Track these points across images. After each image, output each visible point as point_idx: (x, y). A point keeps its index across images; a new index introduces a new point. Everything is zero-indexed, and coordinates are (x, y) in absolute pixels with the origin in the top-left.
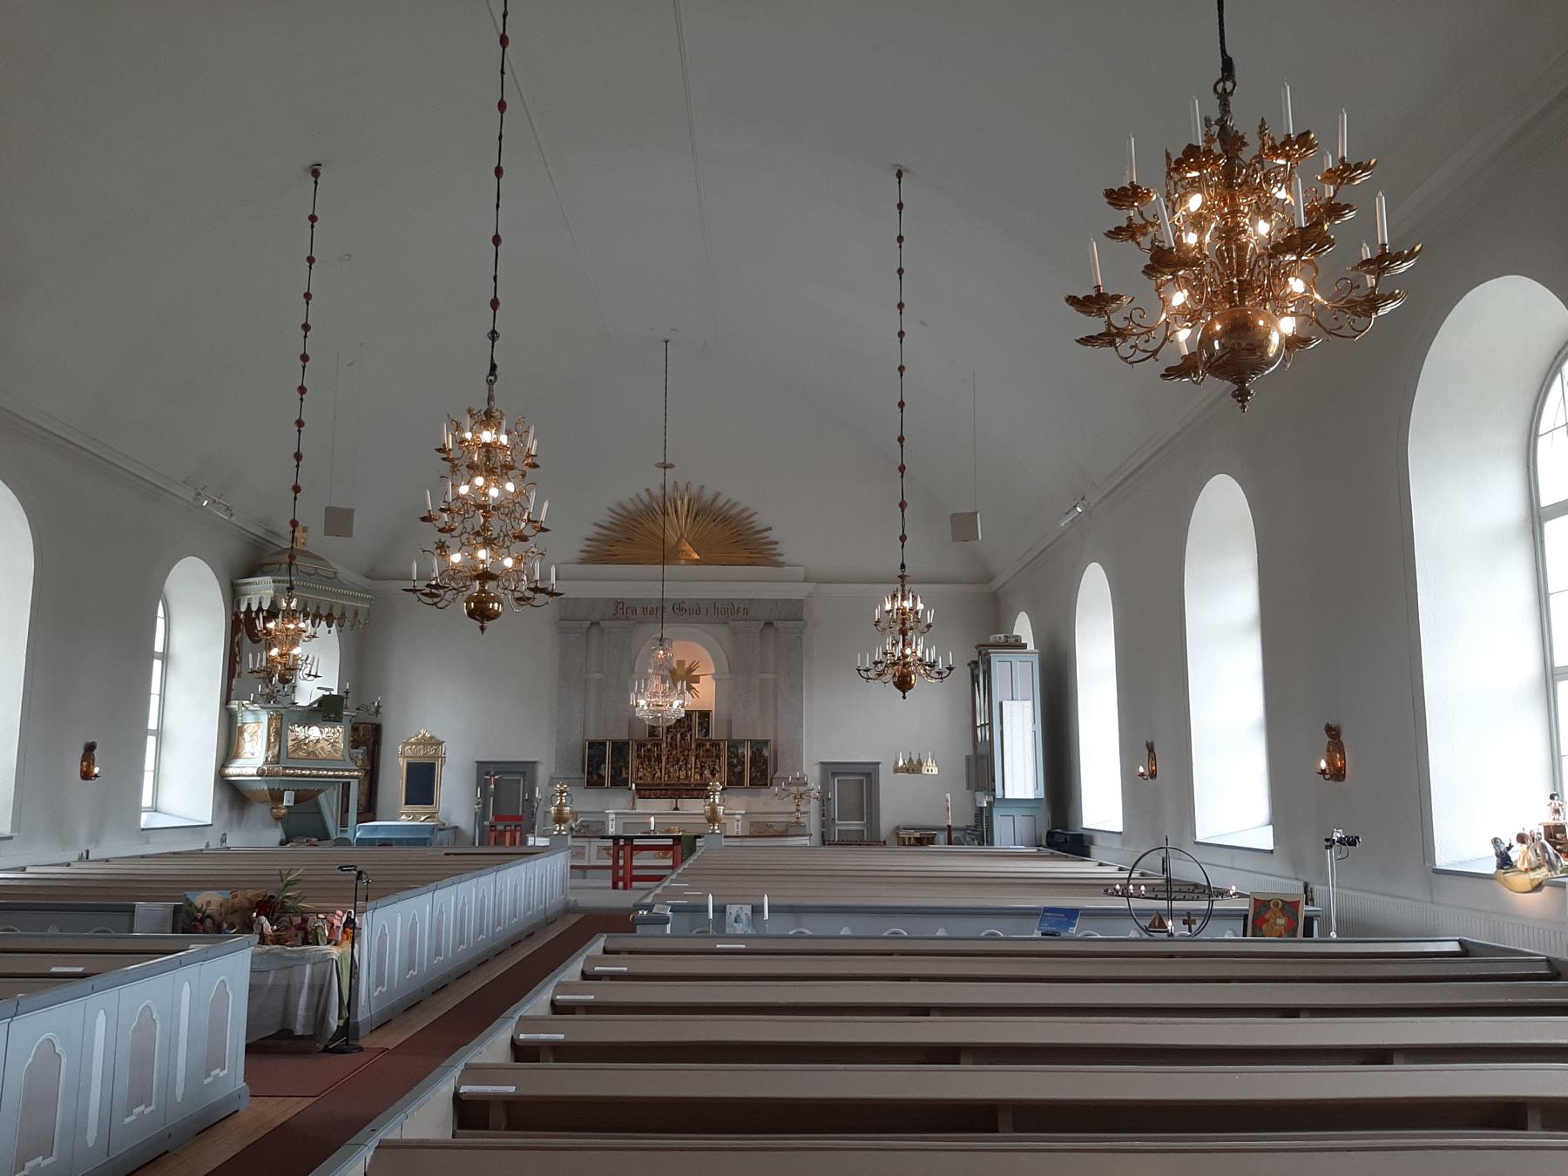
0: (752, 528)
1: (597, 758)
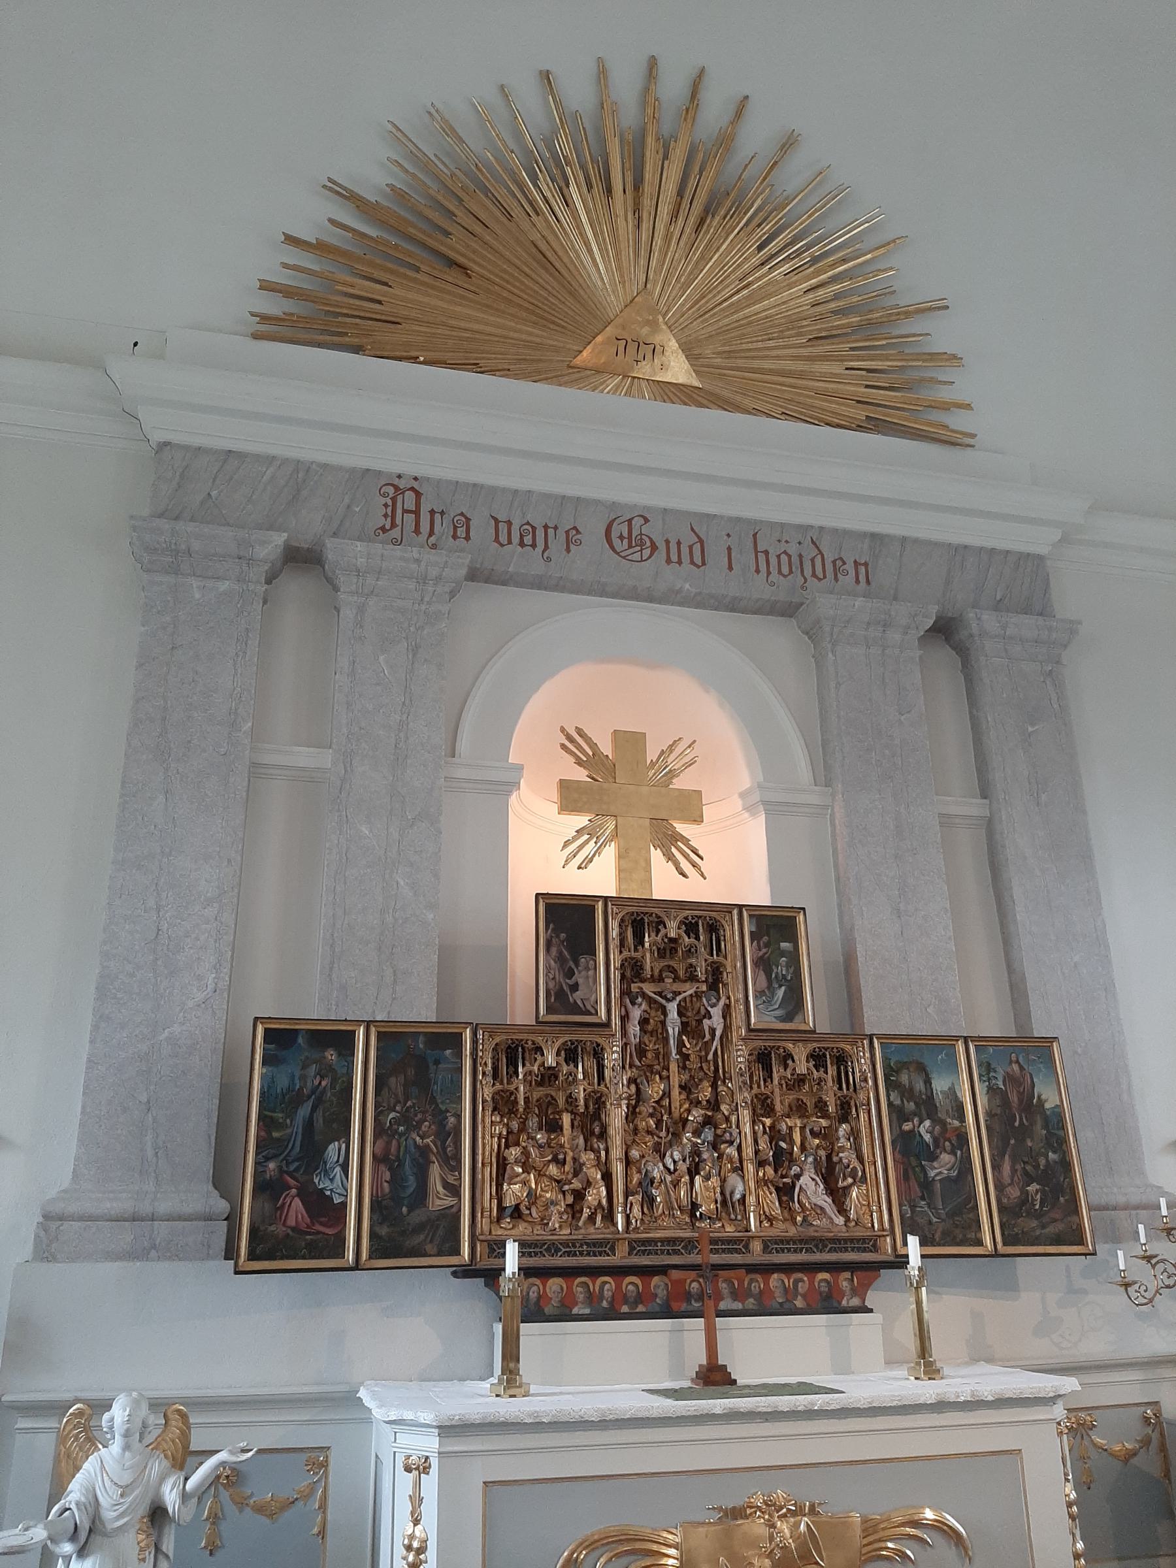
1: (304, 1111)
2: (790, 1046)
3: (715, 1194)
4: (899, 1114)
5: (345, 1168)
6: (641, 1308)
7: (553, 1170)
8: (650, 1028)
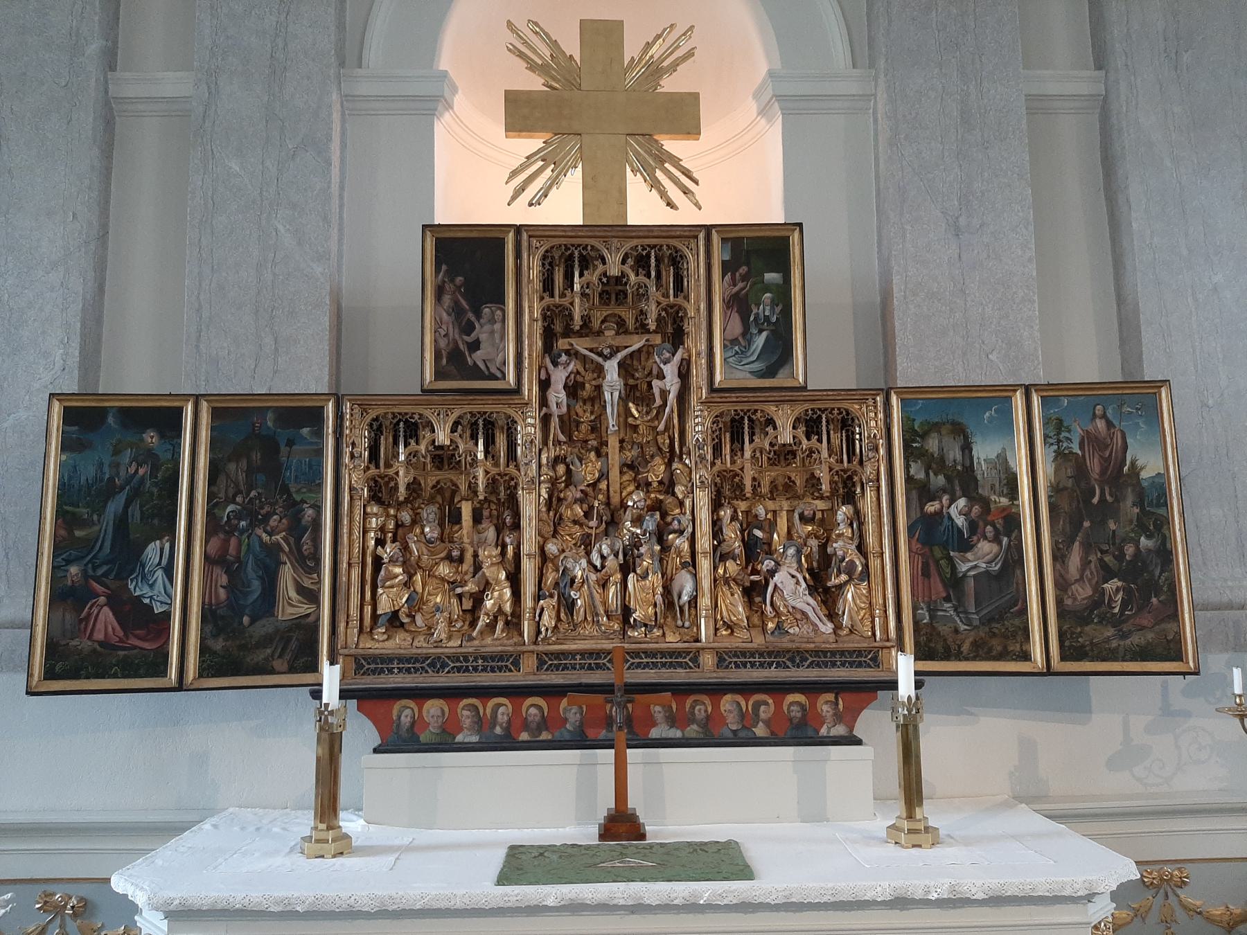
1: (114, 507)
2: (772, 409)
3: (654, 596)
4: (920, 491)
5: (169, 571)
6: (545, 736)
7: (444, 570)
8: (585, 394)
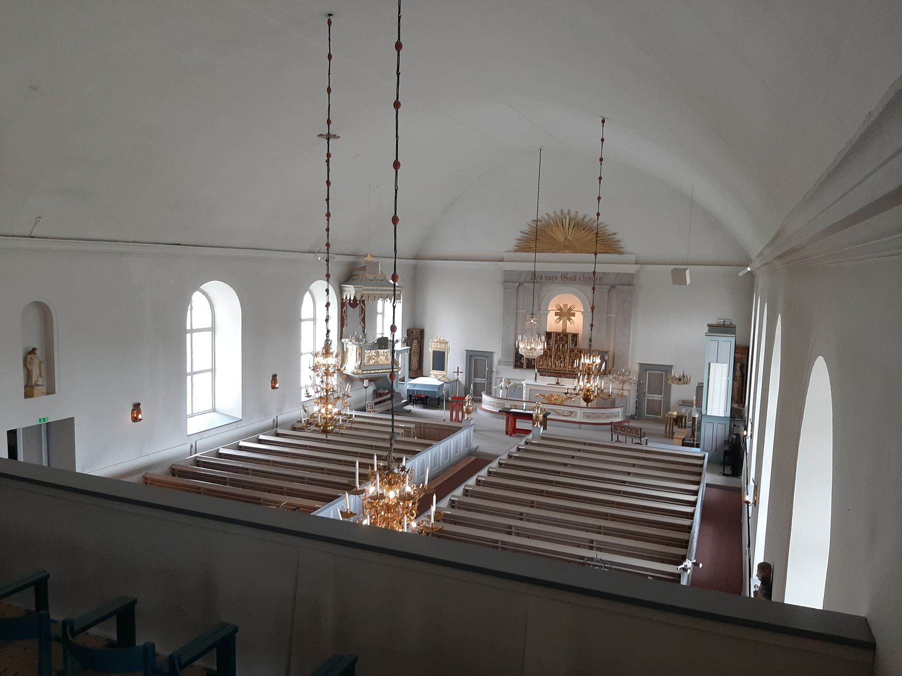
0: (606, 233)
